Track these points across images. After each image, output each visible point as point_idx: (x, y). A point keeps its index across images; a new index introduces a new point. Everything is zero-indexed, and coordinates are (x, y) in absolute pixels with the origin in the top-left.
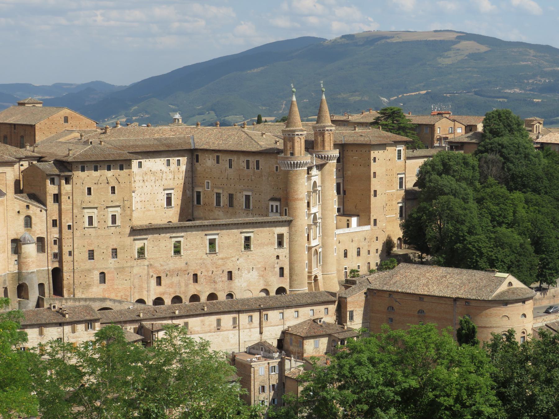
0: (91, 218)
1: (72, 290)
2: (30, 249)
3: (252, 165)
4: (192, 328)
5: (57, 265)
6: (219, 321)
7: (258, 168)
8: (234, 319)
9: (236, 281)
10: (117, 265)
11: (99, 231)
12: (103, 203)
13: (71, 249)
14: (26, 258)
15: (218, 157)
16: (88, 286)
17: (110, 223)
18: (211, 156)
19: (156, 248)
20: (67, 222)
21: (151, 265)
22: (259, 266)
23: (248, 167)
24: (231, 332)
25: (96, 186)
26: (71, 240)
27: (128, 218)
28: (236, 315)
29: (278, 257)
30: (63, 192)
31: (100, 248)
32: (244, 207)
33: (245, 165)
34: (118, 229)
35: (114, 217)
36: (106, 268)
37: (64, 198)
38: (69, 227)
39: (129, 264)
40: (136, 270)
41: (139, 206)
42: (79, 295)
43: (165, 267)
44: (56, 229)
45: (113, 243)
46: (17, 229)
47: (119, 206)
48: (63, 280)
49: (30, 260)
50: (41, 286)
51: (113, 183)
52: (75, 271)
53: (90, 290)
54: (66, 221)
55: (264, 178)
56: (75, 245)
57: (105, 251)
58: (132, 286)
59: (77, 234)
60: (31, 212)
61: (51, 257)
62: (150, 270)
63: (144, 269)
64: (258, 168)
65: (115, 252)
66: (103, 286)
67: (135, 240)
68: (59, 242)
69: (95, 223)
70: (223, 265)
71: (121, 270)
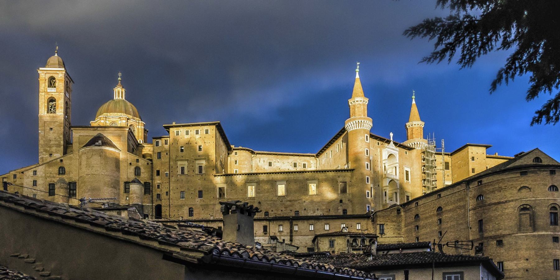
0: (183, 169)
10: (203, 203)
11: (189, 178)
12: (192, 157)
13: (168, 190)
19: (233, 191)
20: (165, 171)
22: (324, 208)
26: (168, 184)
29: (341, 201)
39: (212, 203)
52: (171, 206)
56: (171, 188)
59: (173, 179)
65: (200, 194)
69: (186, 172)
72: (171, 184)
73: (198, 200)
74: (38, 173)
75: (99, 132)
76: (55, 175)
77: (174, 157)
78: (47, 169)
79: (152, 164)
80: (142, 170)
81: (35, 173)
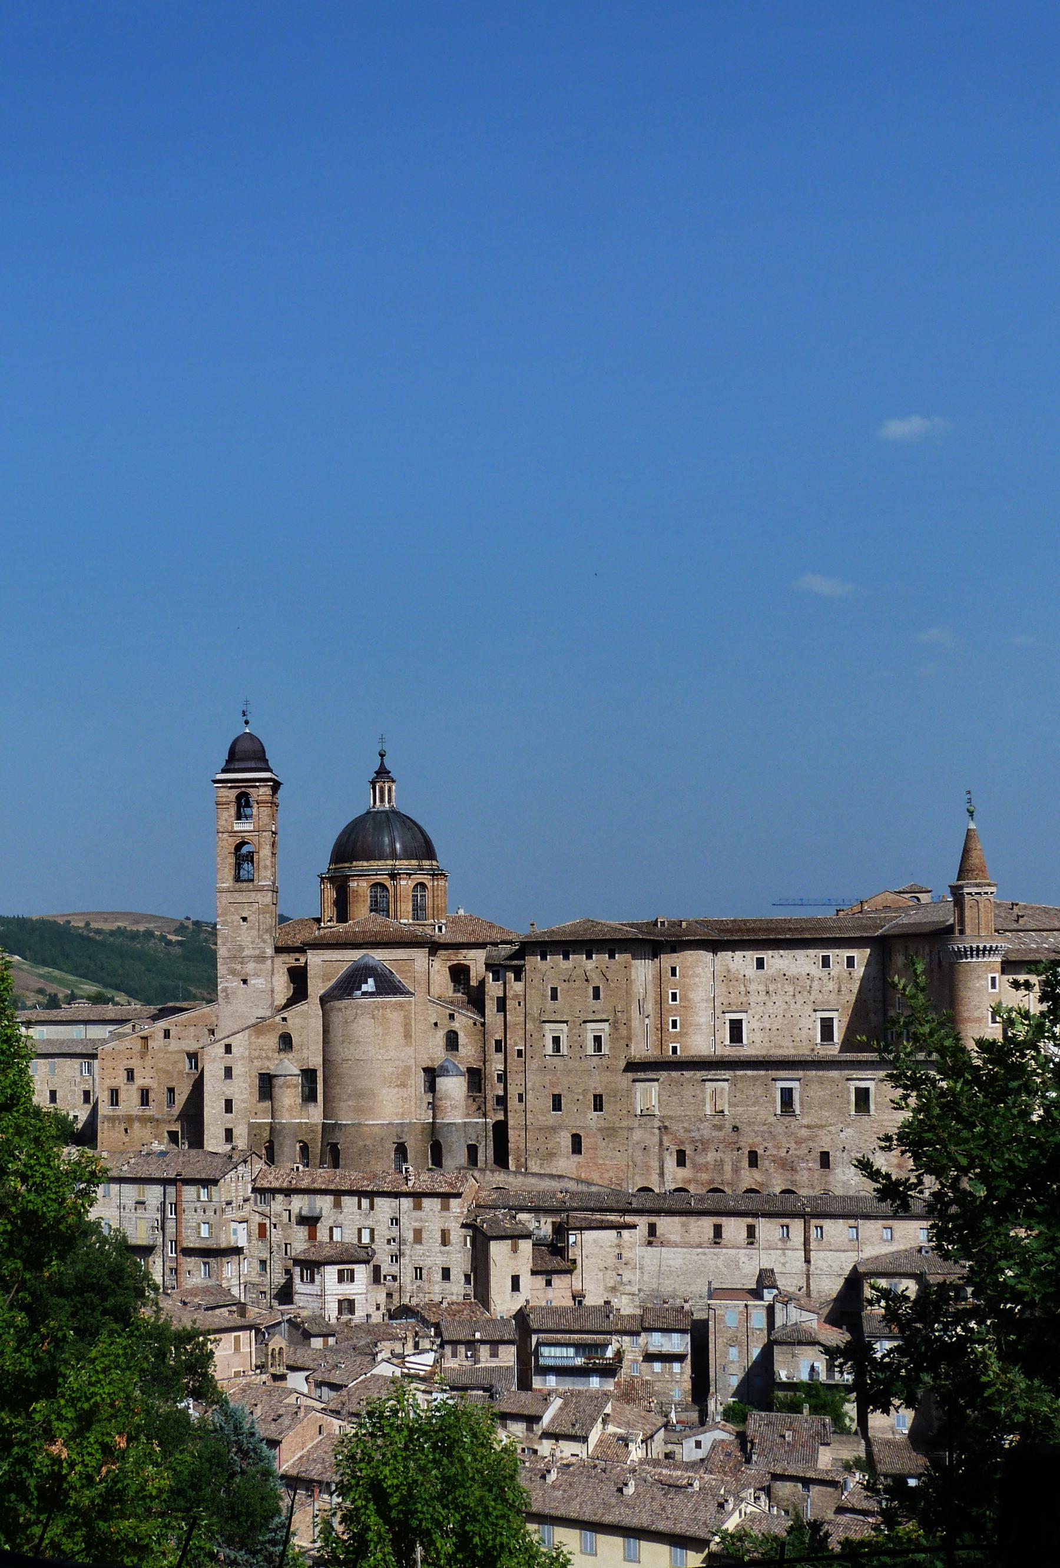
0: (556, 1040)
1: (523, 1160)
2: (454, 1087)
4: (663, 1235)
5: (501, 1117)
6: (718, 1230)
10: (603, 1124)
11: (572, 1064)
13: (522, 1090)
14: (440, 1099)
16: (551, 1155)
17: (590, 1049)
19: (675, 1098)
21: (666, 1128)
24: (744, 1251)
25: (565, 985)
27: (623, 1042)
28: (750, 1220)
30: (510, 994)
34: (605, 1062)
35: (597, 1039)
36: (583, 1128)
37: (510, 1004)
38: (520, 1052)
39: (624, 1124)
40: (637, 1135)
41: (758, 1037)
42: (534, 1166)
43: (693, 1134)
44: (501, 1056)
45: (596, 1084)
46: (435, 1050)
47: (607, 1021)
48: (508, 1141)
49: (449, 1103)
50: (472, 1150)
51: (597, 981)
53: (554, 1163)
54: (515, 1043)
57: (581, 1097)
58: (631, 1163)
59: (533, 1064)
60: (457, 1025)
61: (491, 1103)
62: (665, 1138)
63: (654, 1134)
65: (598, 1103)
66: (576, 1158)
67: (634, 1081)
69: (564, 1049)
71: (609, 1132)
77: (536, 1012)
79: (483, 1024)
80: (462, 1039)
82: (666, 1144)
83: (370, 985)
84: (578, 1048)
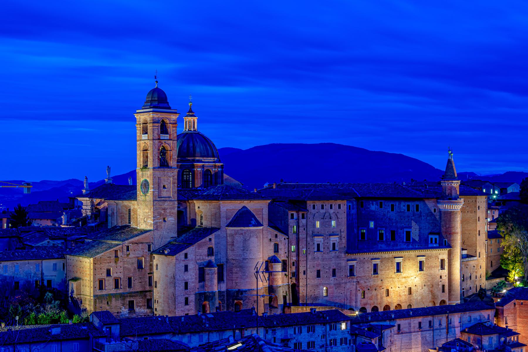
0: (318, 245)
3: (413, 208)
5: (294, 281)
7: (417, 210)
8: (430, 322)
9: (414, 295)
10: (336, 282)
11: (324, 255)
13: (305, 269)
15: (381, 203)
18: (374, 202)
19: (361, 269)
21: (358, 282)
22: (429, 284)
23: (408, 210)
26: (305, 262)
30: (301, 225)
31: (325, 268)
32: (405, 241)
33: (406, 208)
39: (343, 281)
48: (299, 293)
55: (423, 218)
56: (308, 266)
62: (358, 286)
63: (354, 285)
64: (417, 210)
68: (297, 264)
69: (321, 249)
70: (406, 282)
72: (308, 263)
73: (332, 278)
74: (189, 256)
75: (243, 205)
76: (204, 257)
77: (311, 233)
78: (197, 250)
79: (288, 238)
81: (186, 256)
82: (358, 289)
83: (253, 222)
84: (327, 249)
